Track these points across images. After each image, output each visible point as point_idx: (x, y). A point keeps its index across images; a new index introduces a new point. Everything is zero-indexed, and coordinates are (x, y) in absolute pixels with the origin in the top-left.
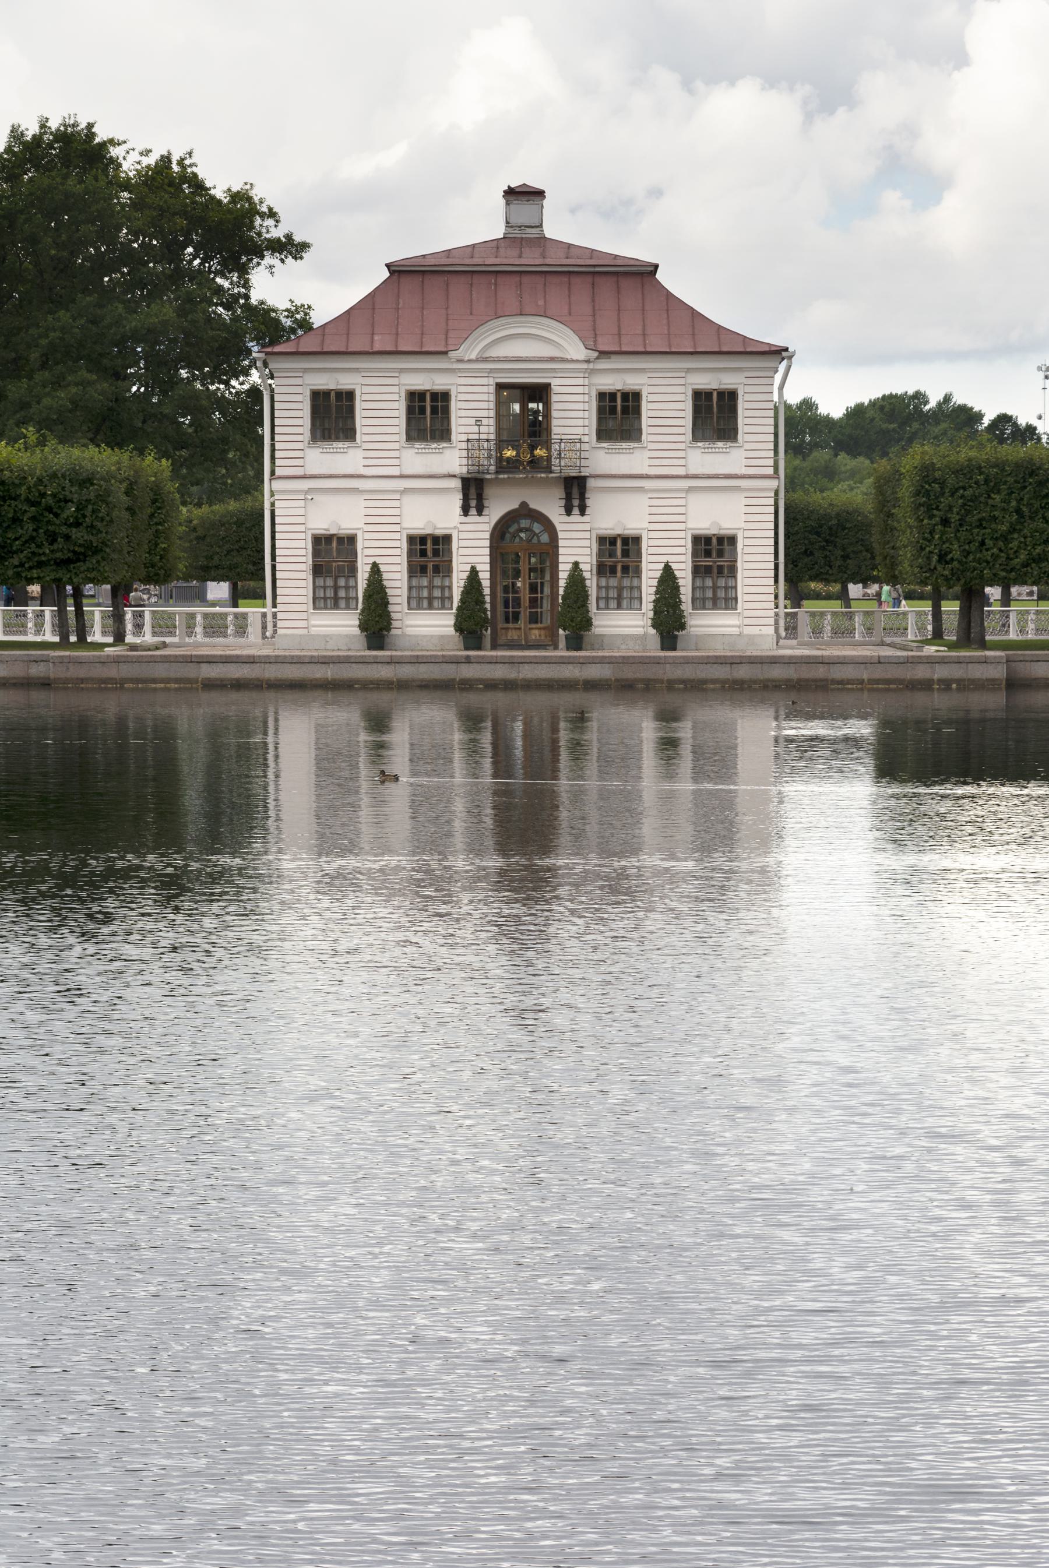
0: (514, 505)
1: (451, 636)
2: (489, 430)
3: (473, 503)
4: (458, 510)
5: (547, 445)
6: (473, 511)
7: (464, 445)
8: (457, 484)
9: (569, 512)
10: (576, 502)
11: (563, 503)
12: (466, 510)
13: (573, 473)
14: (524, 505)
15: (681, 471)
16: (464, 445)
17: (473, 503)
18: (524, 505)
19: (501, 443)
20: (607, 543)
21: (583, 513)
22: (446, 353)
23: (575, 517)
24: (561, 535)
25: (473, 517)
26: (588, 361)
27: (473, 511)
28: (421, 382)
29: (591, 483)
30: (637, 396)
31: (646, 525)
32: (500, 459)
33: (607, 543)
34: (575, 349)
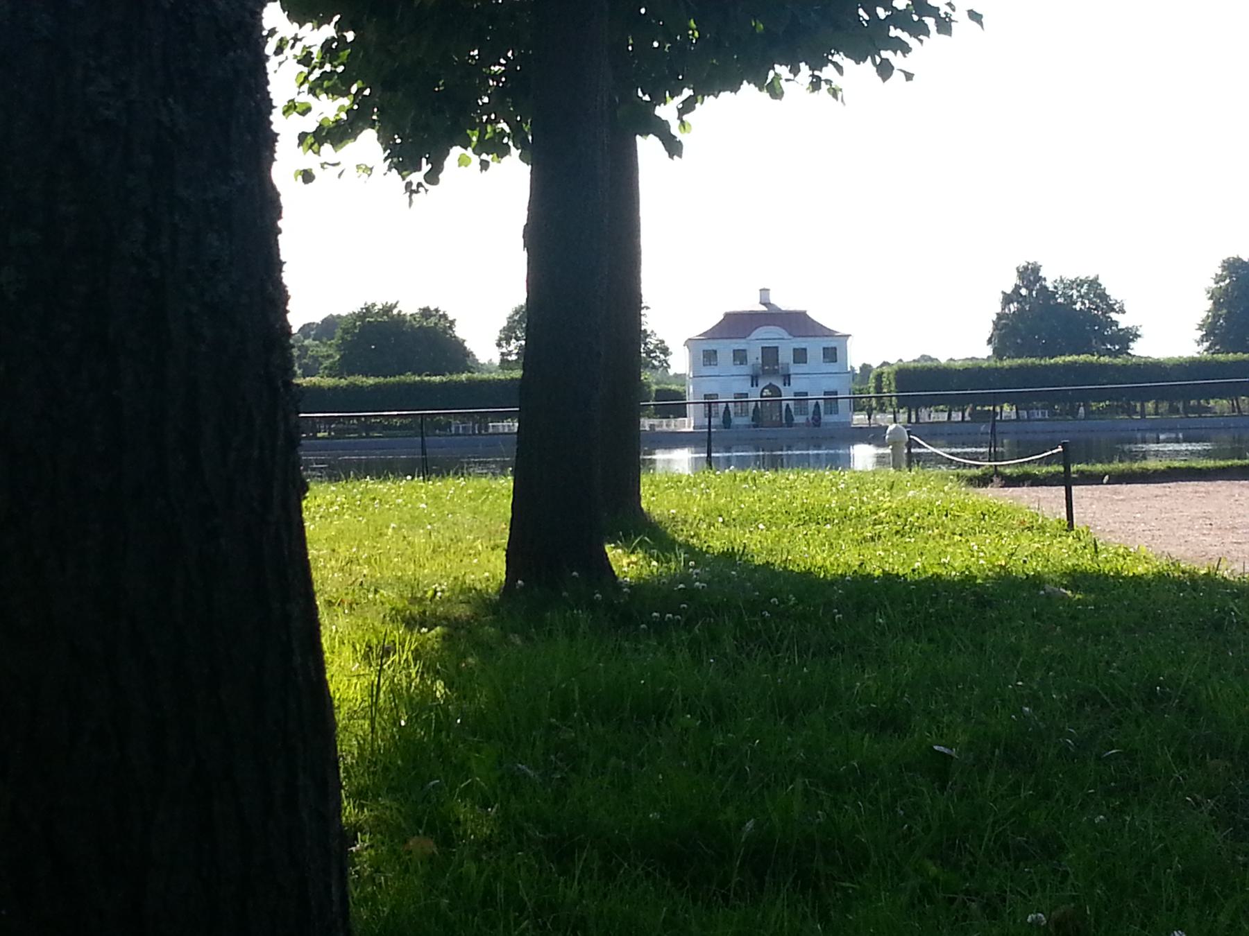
0: (768, 383)
2: (760, 361)
3: (755, 384)
4: (750, 384)
5: (778, 364)
8: (749, 378)
9: (785, 385)
10: (787, 382)
12: (752, 386)
13: (786, 373)
14: (770, 384)
17: (755, 384)
18: (770, 384)
19: (763, 365)
21: (789, 384)
22: (745, 338)
23: (787, 387)
25: (755, 387)
28: (736, 347)
29: (792, 376)
30: (805, 350)
32: (763, 370)
34: (786, 335)
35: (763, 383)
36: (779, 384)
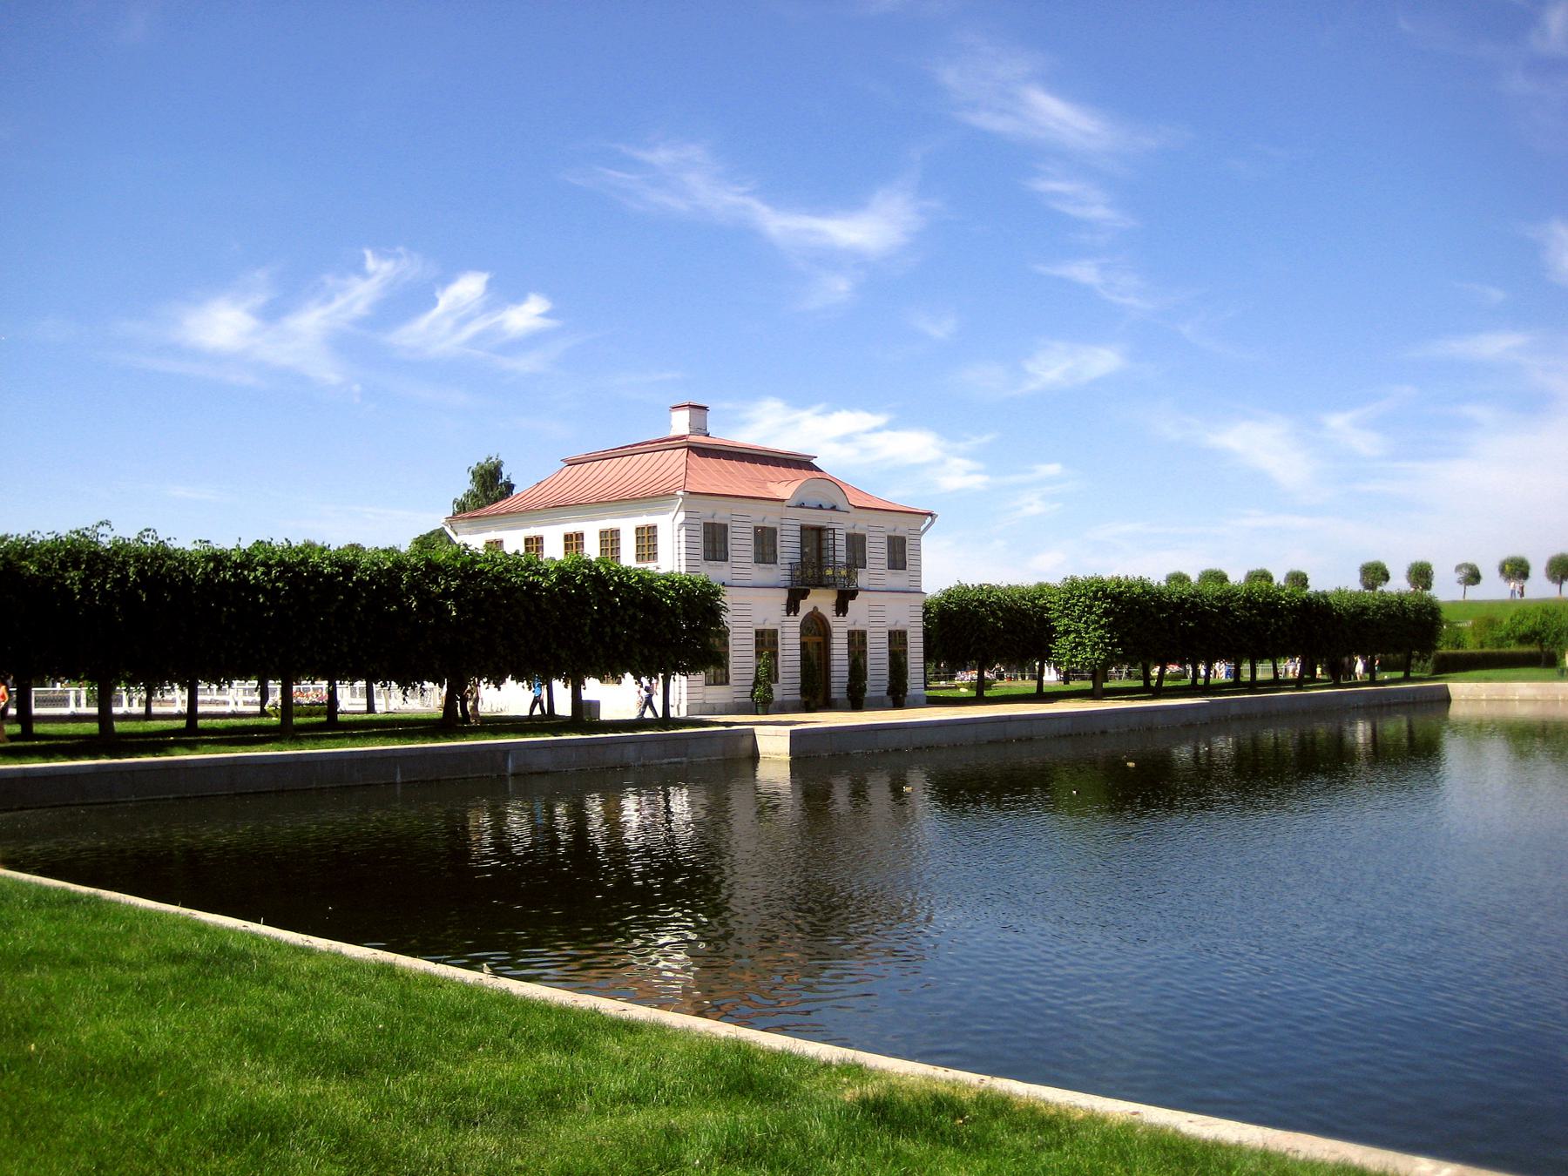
1: (844, 699)
6: (792, 614)
7: (788, 567)
9: (838, 615)
11: (834, 608)
14: (815, 608)
15: (884, 588)
16: (788, 567)
18: (815, 608)
20: (851, 634)
23: (841, 618)
24: (834, 630)
25: (792, 618)
26: (848, 512)
27: (792, 614)
31: (867, 622)
33: (851, 634)
35: (805, 607)
36: (827, 611)
